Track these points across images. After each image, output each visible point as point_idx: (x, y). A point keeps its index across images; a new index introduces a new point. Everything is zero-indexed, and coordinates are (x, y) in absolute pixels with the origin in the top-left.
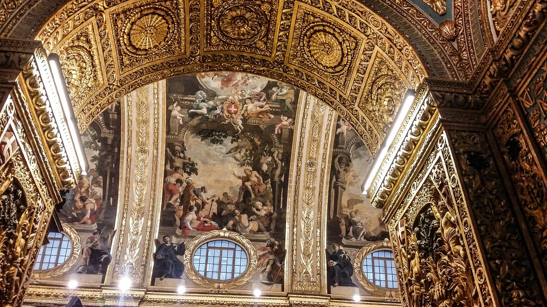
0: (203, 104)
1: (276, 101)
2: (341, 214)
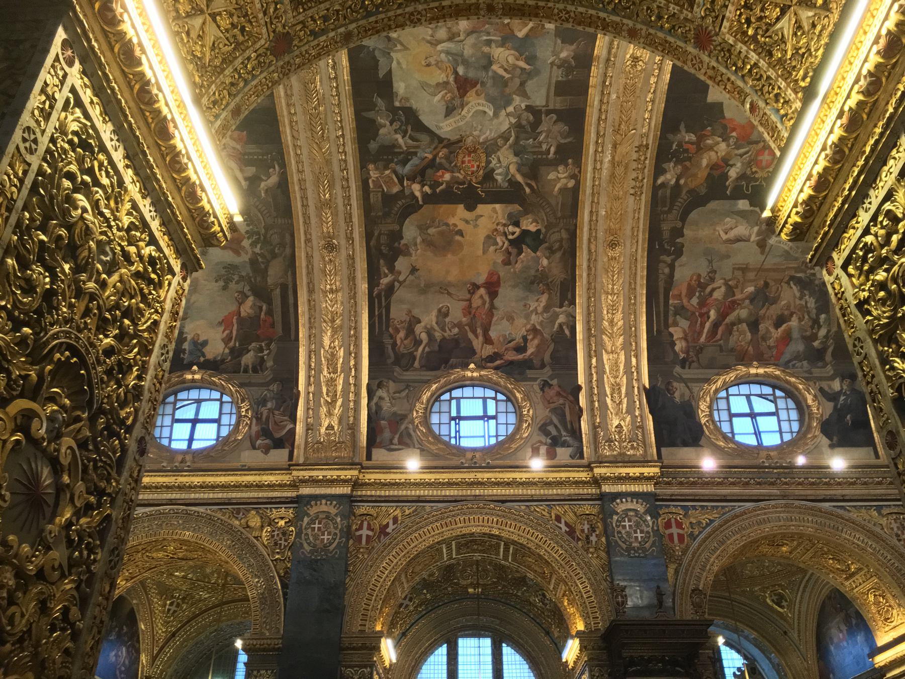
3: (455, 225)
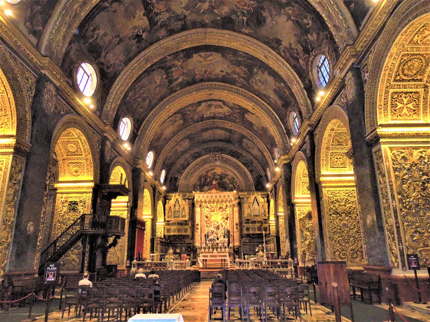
0: (240, 17)
3: (136, 14)
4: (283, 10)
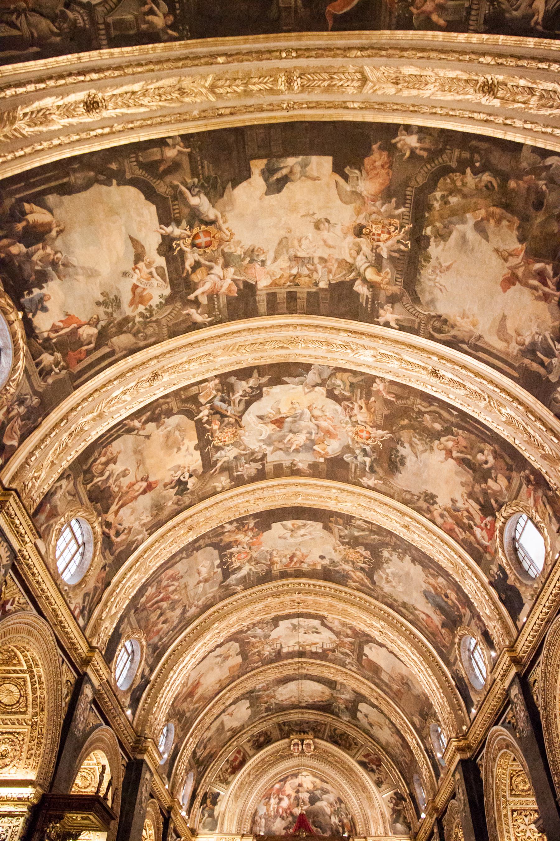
0: (359, 458)
1: (352, 392)
2: (515, 358)
4: (437, 442)
